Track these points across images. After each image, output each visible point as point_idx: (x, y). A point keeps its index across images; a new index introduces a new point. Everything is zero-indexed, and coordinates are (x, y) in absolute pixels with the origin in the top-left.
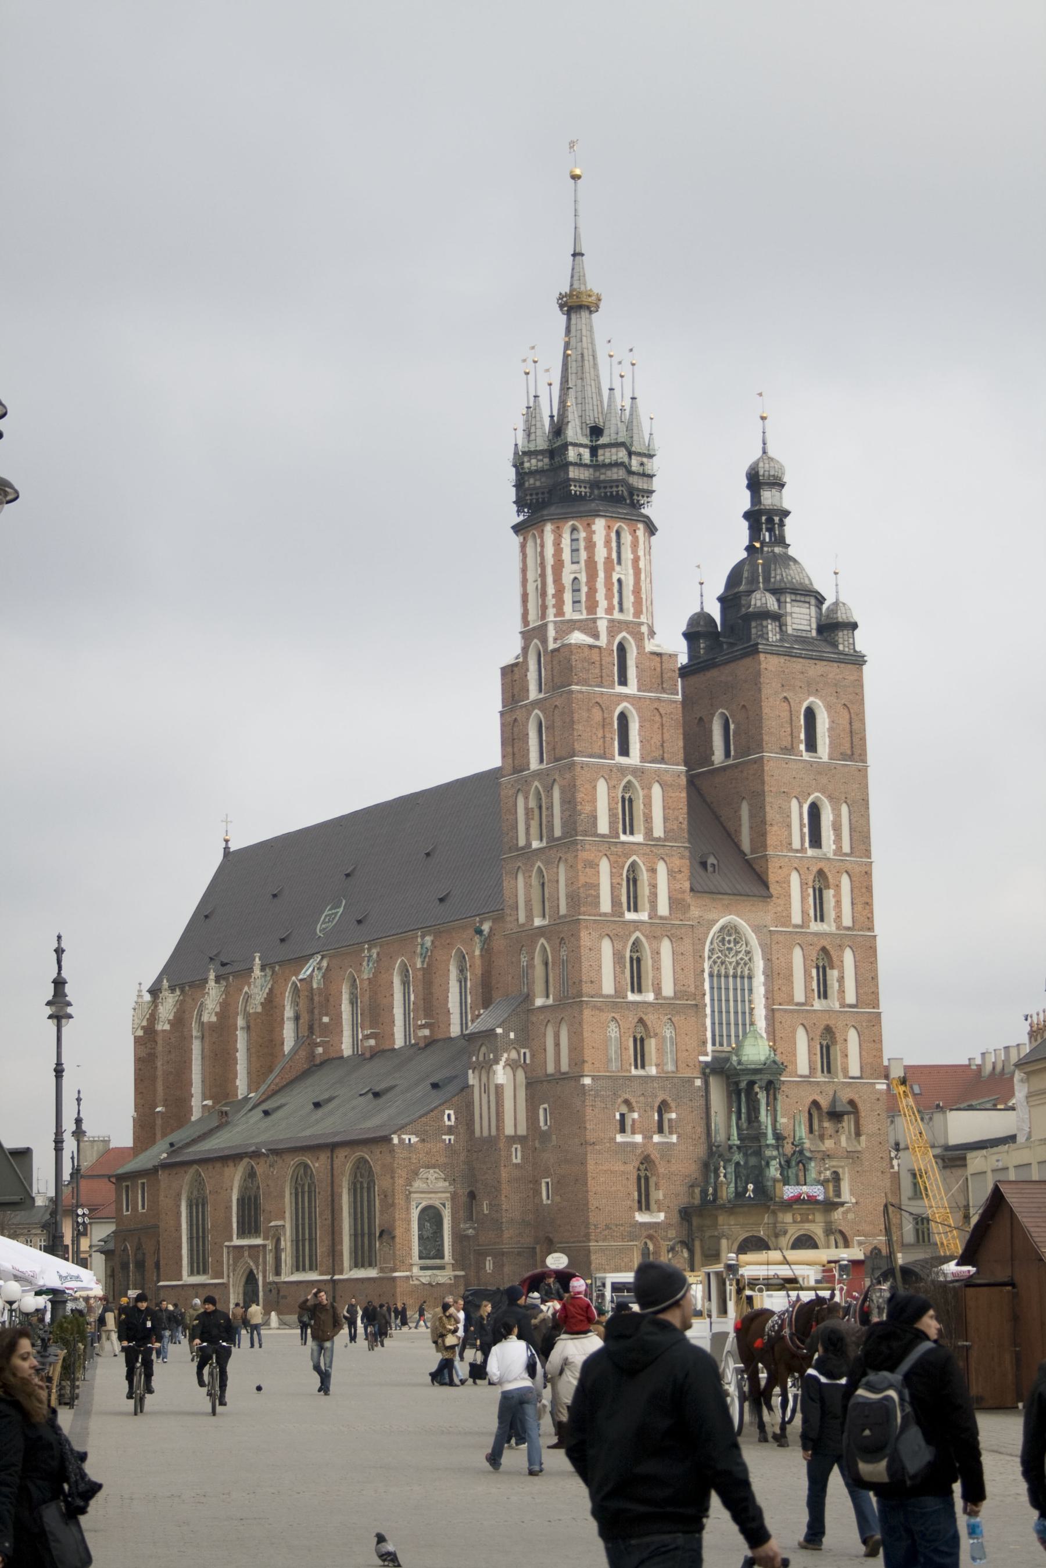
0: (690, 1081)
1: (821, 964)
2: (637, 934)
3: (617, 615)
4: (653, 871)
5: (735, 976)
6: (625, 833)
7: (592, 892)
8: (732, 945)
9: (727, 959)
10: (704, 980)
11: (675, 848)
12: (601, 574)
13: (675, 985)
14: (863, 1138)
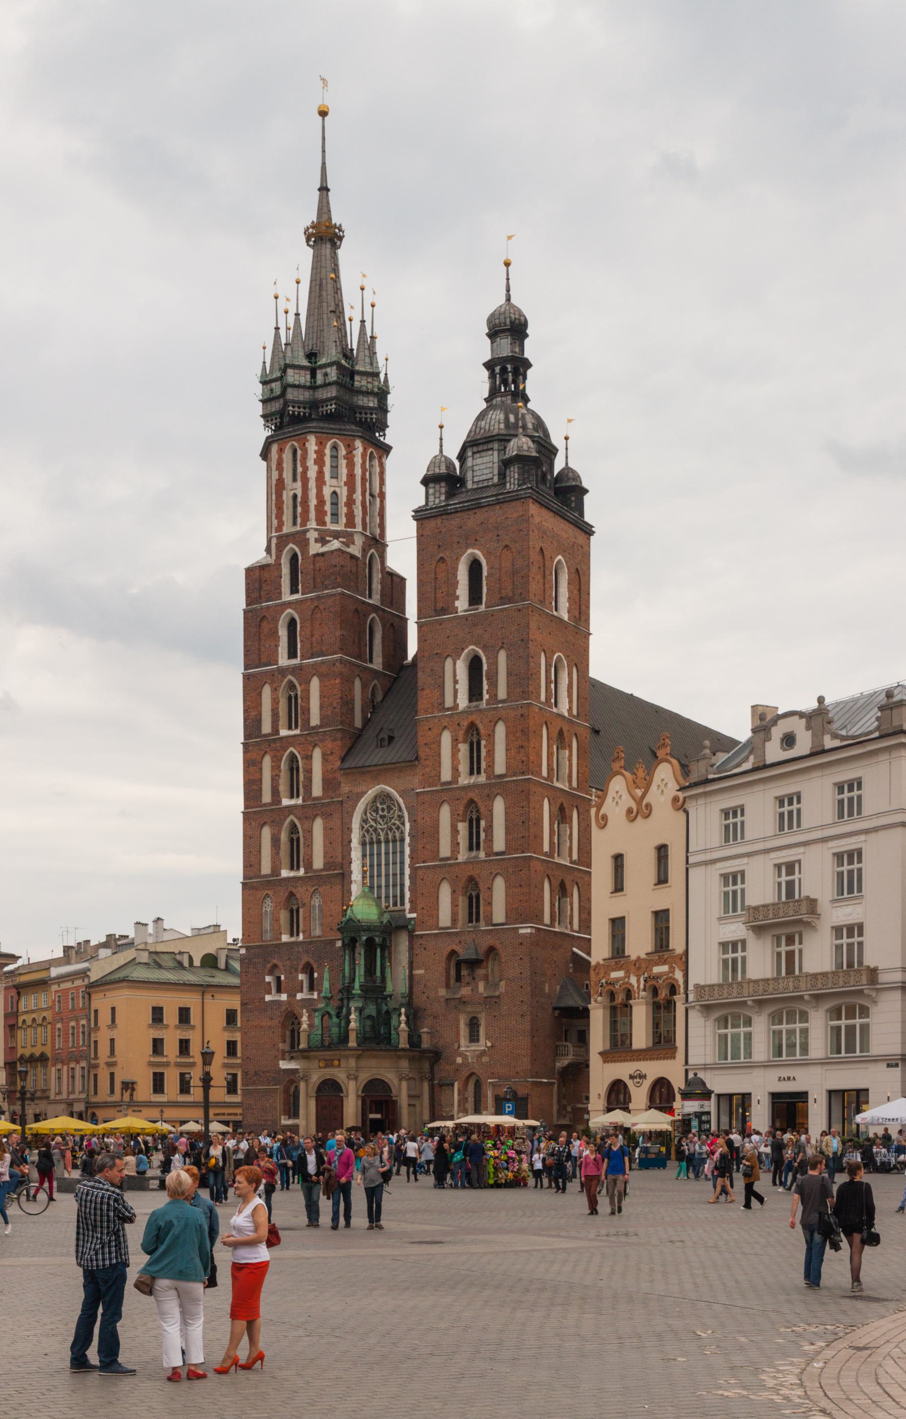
0: (332, 942)
1: (474, 817)
2: (292, 817)
3: (287, 529)
4: (308, 758)
5: (387, 842)
6: (290, 728)
7: (254, 787)
8: (385, 813)
9: (379, 826)
10: (351, 849)
11: (328, 733)
12: (274, 497)
13: (325, 857)
14: (503, 983)
